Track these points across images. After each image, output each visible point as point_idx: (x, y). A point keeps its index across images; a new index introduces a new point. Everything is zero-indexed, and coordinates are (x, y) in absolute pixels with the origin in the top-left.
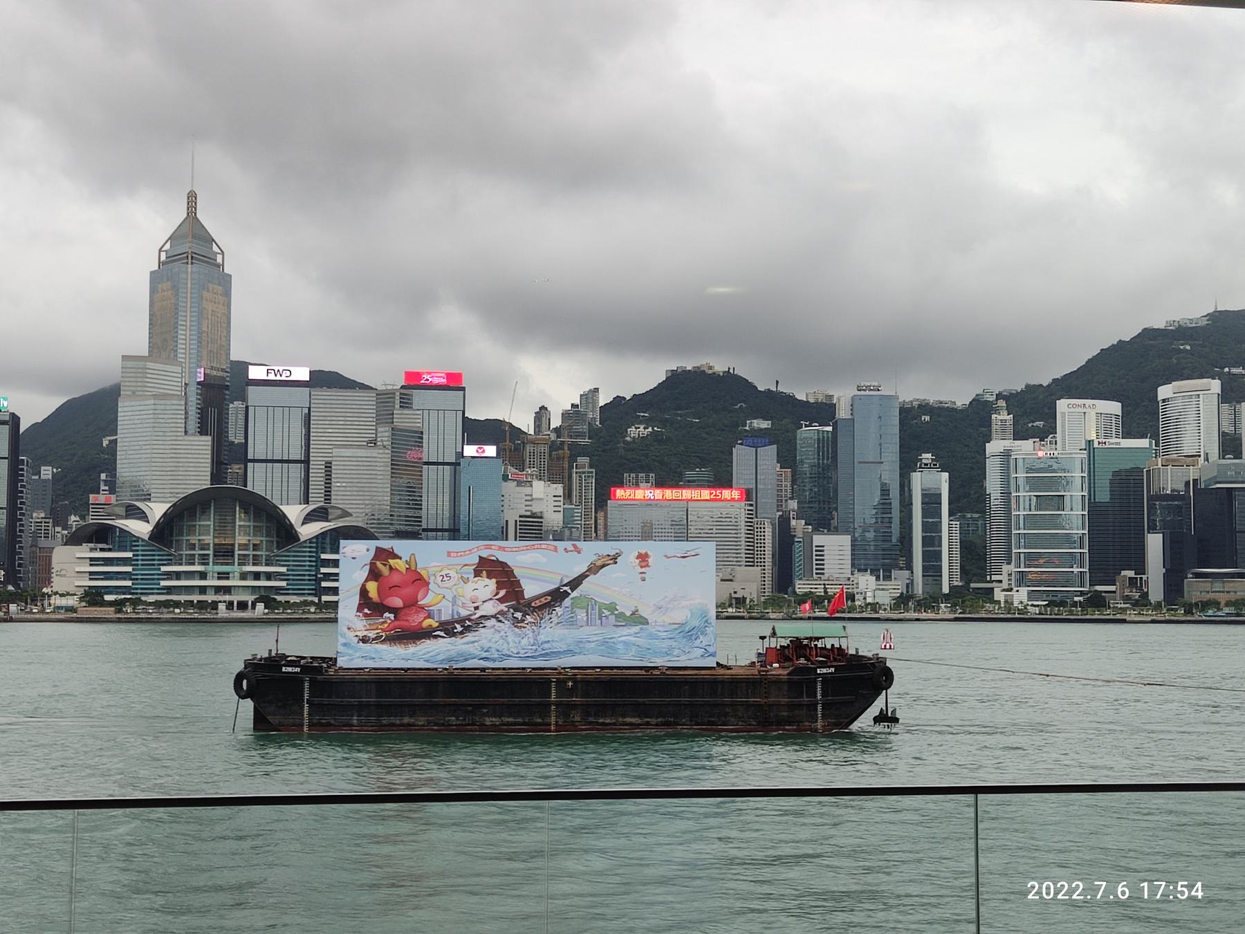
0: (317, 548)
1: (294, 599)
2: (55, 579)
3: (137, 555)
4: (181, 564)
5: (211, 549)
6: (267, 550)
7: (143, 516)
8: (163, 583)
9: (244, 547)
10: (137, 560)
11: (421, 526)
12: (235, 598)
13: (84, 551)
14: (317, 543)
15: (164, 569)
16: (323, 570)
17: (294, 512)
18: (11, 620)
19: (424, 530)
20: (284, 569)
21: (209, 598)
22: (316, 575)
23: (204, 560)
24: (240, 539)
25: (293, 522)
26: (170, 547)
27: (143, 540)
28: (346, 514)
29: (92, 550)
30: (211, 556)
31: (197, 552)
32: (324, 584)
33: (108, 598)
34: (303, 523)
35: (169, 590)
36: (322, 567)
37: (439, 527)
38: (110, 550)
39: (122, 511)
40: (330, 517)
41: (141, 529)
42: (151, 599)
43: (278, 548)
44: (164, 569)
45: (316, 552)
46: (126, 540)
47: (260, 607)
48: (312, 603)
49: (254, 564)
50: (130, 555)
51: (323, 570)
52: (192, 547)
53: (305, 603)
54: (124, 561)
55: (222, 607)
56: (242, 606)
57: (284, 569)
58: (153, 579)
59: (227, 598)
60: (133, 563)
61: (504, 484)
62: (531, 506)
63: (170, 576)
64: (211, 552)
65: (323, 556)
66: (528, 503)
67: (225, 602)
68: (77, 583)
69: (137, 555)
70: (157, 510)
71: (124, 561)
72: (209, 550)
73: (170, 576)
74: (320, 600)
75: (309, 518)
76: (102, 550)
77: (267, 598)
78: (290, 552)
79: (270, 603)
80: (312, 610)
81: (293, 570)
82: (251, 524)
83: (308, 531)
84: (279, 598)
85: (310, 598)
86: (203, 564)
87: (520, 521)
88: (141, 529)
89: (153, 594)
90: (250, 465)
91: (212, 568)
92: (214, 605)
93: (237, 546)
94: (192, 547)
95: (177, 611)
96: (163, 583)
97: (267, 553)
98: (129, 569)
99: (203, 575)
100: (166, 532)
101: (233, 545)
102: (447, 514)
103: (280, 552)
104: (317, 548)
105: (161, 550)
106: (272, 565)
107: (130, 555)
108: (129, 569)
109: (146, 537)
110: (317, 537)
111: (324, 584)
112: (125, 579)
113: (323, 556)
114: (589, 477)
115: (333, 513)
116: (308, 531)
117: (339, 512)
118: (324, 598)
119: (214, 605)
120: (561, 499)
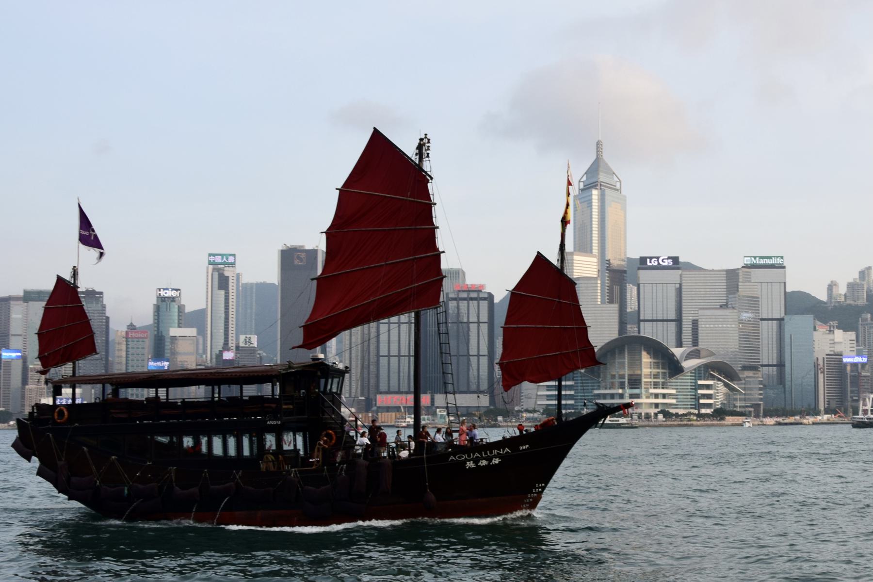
0: (695, 376)
2: (524, 400)
3: (577, 383)
5: (626, 378)
6: (663, 378)
9: (646, 376)
10: (577, 386)
11: (759, 362)
14: (695, 373)
16: (700, 392)
19: (763, 366)
22: (695, 395)
23: (622, 386)
24: (646, 371)
28: (712, 354)
30: (626, 383)
32: (702, 401)
34: (685, 360)
36: (699, 389)
37: (771, 363)
43: (671, 377)
45: (695, 379)
47: (660, 417)
51: (700, 392)
52: (613, 376)
57: (674, 391)
60: (575, 388)
61: (815, 332)
62: (834, 347)
65: (700, 382)
66: (832, 345)
67: (636, 413)
68: (539, 403)
69: (577, 383)
75: (689, 356)
78: (677, 379)
79: (667, 415)
81: (680, 392)
85: (692, 411)
87: (827, 358)
90: (642, 323)
91: (628, 391)
93: (643, 375)
97: (663, 380)
98: (572, 392)
99: (621, 396)
101: (640, 375)
102: (775, 356)
104: (695, 376)
106: (667, 388)
111: (702, 401)
113: (700, 382)
114: (870, 327)
120: (855, 342)
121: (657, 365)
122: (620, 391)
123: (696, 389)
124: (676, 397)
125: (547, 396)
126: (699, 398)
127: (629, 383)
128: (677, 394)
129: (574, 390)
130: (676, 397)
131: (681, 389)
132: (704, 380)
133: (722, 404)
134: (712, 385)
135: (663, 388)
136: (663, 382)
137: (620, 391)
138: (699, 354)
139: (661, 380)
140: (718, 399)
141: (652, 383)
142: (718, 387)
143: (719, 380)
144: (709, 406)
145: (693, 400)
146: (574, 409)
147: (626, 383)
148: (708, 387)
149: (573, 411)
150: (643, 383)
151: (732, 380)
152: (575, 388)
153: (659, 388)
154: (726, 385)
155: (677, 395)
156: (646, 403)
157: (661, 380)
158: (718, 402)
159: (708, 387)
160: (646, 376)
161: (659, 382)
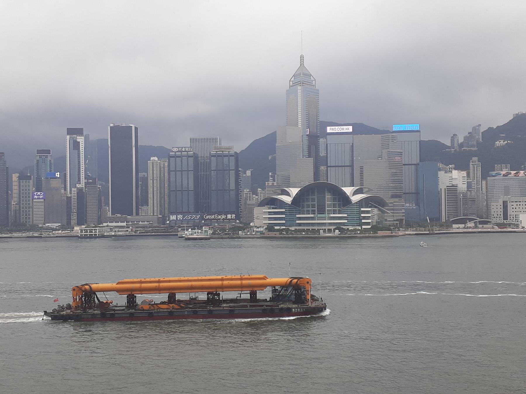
1: (351, 228)
4: (304, 214)
7: (288, 194)
8: (297, 222)
9: (329, 206)
12: (327, 228)
13: (266, 209)
14: (359, 204)
15: (297, 216)
16: (362, 215)
17: (348, 190)
18: (240, 238)
20: (346, 215)
21: (316, 228)
23: (313, 212)
25: (349, 195)
26: (299, 207)
27: (289, 204)
29: (269, 208)
30: (316, 210)
31: (310, 209)
32: (363, 221)
33: (276, 228)
34: (353, 195)
35: (300, 225)
38: (276, 208)
39: (279, 192)
40: (364, 191)
41: (288, 199)
42: (293, 228)
43: (344, 206)
44: (297, 216)
45: (359, 208)
46: (282, 204)
47: (337, 231)
48: (359, 230)
49: (334, 214)
50: (284, 210)
51: (362, 215)
53: (355, 230)
54: (282, 213)
55: (321, 231)
56: (330, 231)
57: (346, 215)
58: (294, 220)
59: (324, 228)
60: (286, 213)
63: (300, 219)
64: (316, 209)
65: (362, 209)
67: (322, 229)
70: (294, 191)
71: (282, 213)
72: (315, 208)
73: (300, 219)
74: (361, 228)
75: (355, 193)
76: (273, 208)
77: (339, 227)
78: (348, 208)
80: (359, 232)
82: (332, 197)
83: (355, 199)
84: (344, 227)
86: (313, 214)
88: (288, 199)
89: (293, 226)
92: (319, 230)
94: (308, 206)
95: (304, 233)
96: (297, 222)
97: (339, 209)
98: (284, 216)
100: (297, 200)
103: (344, 208)
105: (297, 208)
106: (341, 214)
107: (284, 210)
108: (284, 216)
109: (290, 203)
110: (359, 201)
111: (363, 221)
112: (282, 220)
113: (362, 209)
115: (365, 190)
116: (355, 199)
117: (367, 190)
118: (363, 227)
119: (319, 230)
121: (334, 200)
122: (312, 216)
123: (360, 214)
124: (347, 219)
125: (269, 218)
126: (362, 219)
127: (318, 210)
128: (348, 217)
129: (285, 214)
130: (347, 219)
131: (350, 213)
132: (365, 208)
133: (376, 222)
134: (370, 211)
135: (339, 214)
136: (339, 210)
137: (312, 216)
138: (363, 190)
139: (337, 209)
140: (374, 219)
141: (332, 210)
142: (374, 212)
143: (376, 207)
144: (368, 224)
145: (358, 220)
146: (285, 226)
147: (316, 210)
148: (368, 212)
149: (284, 227)
150: (326, 210)
151: (383, 206)
152: (286, 213)
153: (337, 214)
154: (380, 210)
155: (348, 218)
156: (328, 223)
157: (337, 209)
158: (374, 221)
159: (368, 212)
160: (329, 206)
161: (337, 210)
